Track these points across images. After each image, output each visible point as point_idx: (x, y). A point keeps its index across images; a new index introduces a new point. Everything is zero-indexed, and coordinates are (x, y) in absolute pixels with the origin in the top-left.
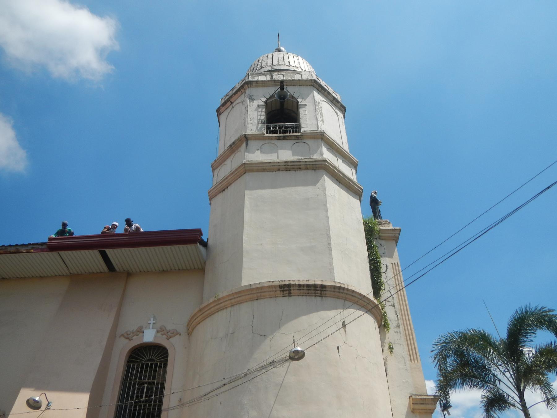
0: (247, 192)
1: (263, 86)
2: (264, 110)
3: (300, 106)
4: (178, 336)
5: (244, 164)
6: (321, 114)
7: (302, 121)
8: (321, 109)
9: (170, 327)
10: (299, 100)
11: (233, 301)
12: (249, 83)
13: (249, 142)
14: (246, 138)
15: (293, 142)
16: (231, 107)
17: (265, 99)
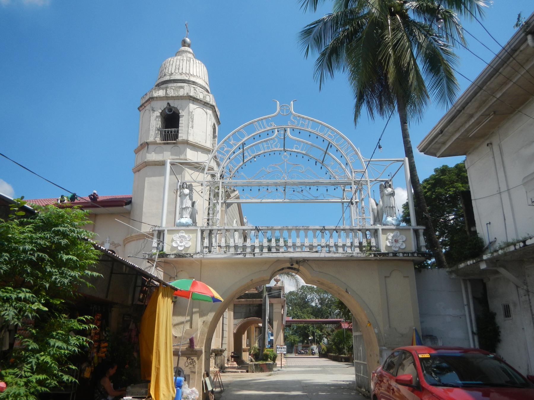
0: (147, 179)
1: (161, 100)
2: (160, 119)
3: (180, 116)
4: (120, 246)
5: (145, 162)
6: (192, 122)
7: (180, 128)
8: (193, 117)
9: (116, 242)
10: (180, 111)
11: (137, 238)
12: (152, 99)
13: (149, 146)
14: (147, 144)
15: (172, 146)
16: (144, 110)
17: (160, 111)
